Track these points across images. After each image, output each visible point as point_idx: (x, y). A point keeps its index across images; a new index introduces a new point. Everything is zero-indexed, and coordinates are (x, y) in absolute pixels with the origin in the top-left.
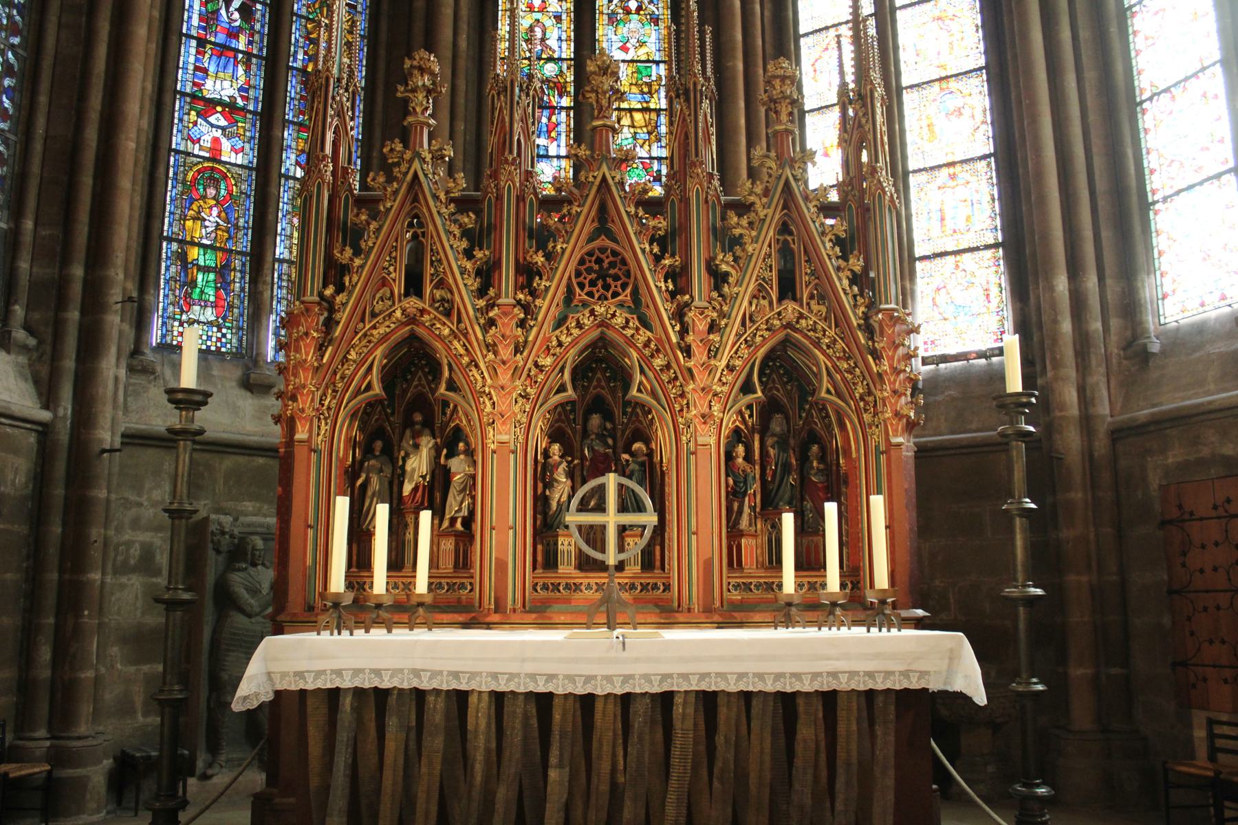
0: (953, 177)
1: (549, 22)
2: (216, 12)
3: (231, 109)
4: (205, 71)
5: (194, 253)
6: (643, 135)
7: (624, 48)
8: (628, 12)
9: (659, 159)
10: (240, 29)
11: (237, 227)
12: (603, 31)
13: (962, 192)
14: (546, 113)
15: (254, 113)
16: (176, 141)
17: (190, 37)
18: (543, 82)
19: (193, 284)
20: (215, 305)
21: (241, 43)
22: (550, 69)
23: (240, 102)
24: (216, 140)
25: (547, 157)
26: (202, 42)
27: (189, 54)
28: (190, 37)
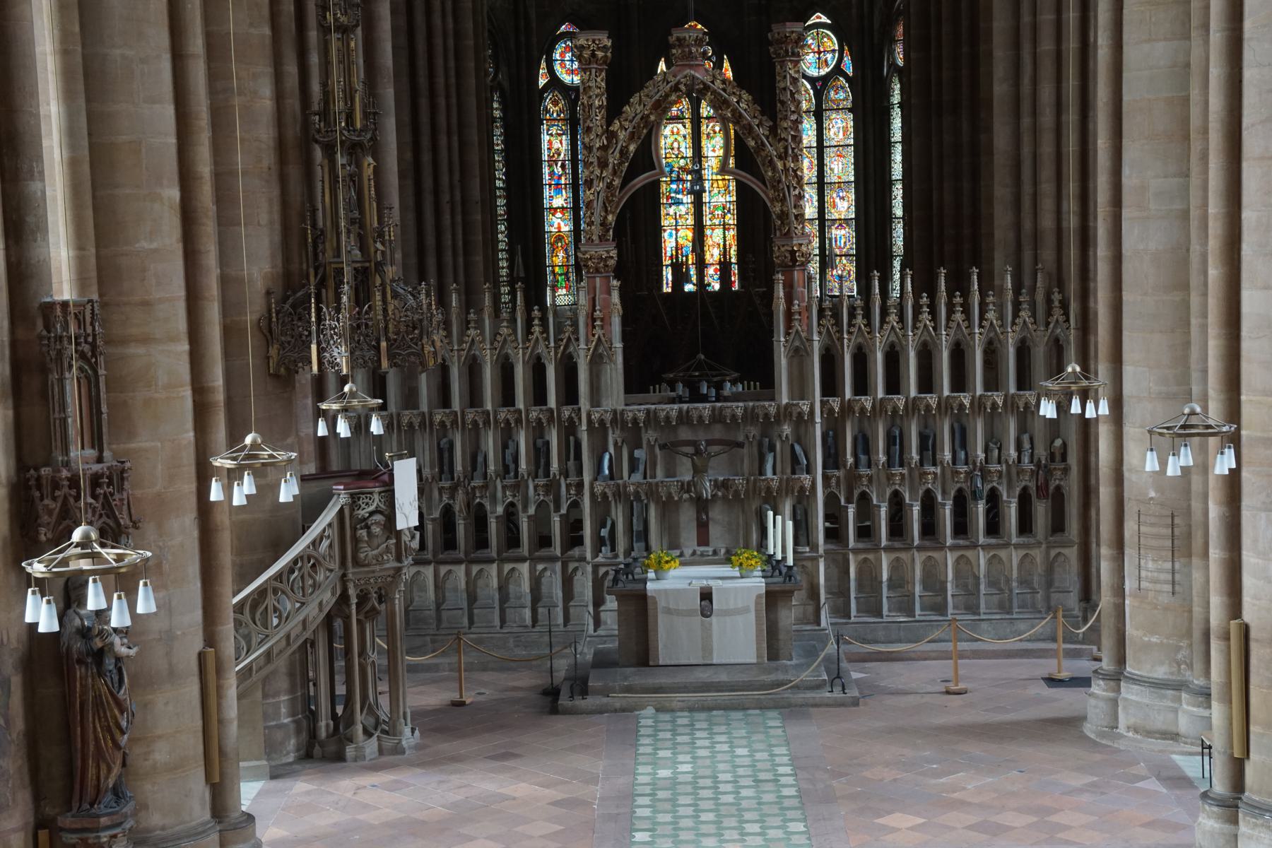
0: (840, 225)
1: (681, 139)
2: (553, 170)
3: (563, 208)
4: (552, 197)
5: (557, 269)
6: (722, 190)
7: (714, 151)
8: (715, 132)
9: (730, 202)
10: (562, 175)
11: (569, 256)
12: (704, 142)
13: (843, 232)
14: (681, 183)
15: (570, 208)
16: (547, 229)
17: (546, 185)
18: (679, 168)
19: (558, 281)
20: (566, 288)
21: (563, 181)
22: (682, 162)
23: (565, 206)
24: (559, 224)
25: (682, 203)
26: (550, 185)
27: (546, 193)
28: (546, 185)
